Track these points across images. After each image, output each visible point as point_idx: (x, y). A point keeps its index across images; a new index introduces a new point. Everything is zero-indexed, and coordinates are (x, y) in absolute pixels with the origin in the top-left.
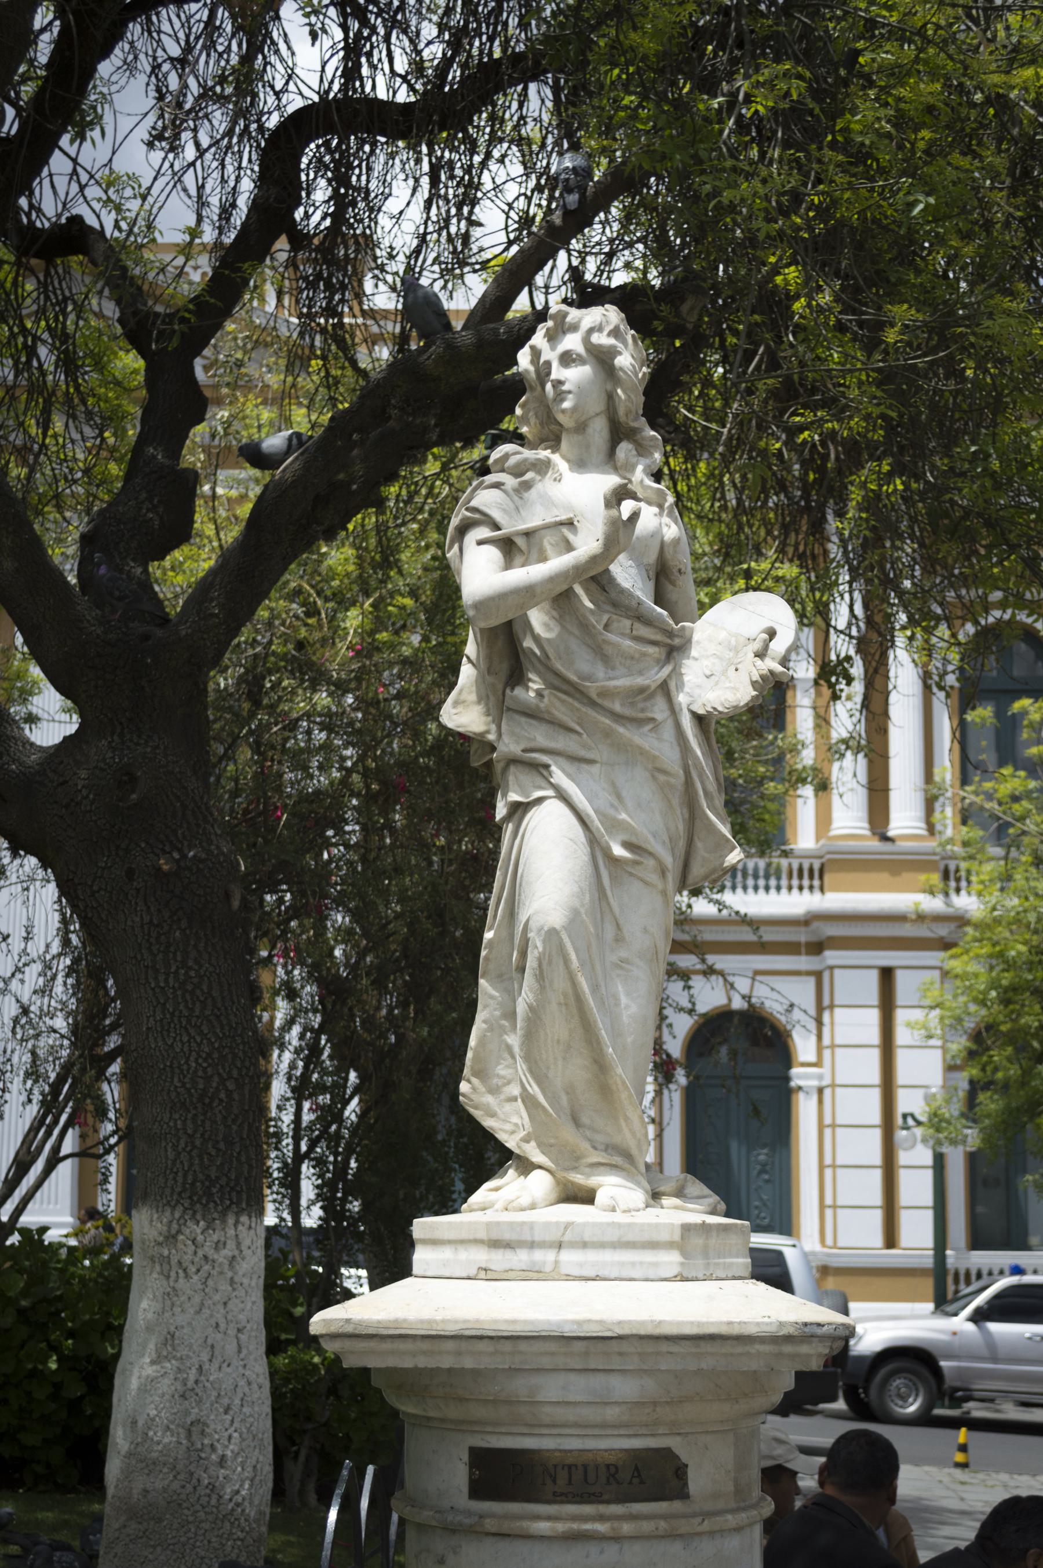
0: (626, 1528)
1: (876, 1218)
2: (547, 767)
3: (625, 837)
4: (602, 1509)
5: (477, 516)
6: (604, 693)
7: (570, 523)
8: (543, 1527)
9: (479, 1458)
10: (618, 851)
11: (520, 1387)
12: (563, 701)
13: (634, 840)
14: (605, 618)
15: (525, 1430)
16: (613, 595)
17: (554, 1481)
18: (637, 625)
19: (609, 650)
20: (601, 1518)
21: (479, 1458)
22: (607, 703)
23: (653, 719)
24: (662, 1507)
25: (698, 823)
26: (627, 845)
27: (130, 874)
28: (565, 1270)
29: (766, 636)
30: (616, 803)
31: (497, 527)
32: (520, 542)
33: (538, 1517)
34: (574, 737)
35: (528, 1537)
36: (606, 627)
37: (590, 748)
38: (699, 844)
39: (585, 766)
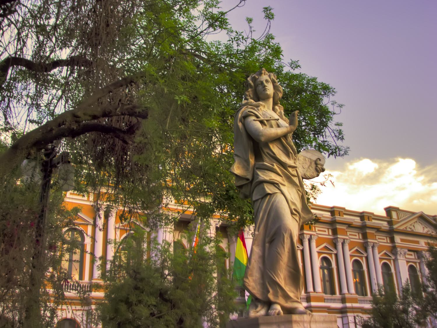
2: (277, 184)
12: (278, 166)
31: (257, 117)
32: (266, 122)
37: (284, 181)
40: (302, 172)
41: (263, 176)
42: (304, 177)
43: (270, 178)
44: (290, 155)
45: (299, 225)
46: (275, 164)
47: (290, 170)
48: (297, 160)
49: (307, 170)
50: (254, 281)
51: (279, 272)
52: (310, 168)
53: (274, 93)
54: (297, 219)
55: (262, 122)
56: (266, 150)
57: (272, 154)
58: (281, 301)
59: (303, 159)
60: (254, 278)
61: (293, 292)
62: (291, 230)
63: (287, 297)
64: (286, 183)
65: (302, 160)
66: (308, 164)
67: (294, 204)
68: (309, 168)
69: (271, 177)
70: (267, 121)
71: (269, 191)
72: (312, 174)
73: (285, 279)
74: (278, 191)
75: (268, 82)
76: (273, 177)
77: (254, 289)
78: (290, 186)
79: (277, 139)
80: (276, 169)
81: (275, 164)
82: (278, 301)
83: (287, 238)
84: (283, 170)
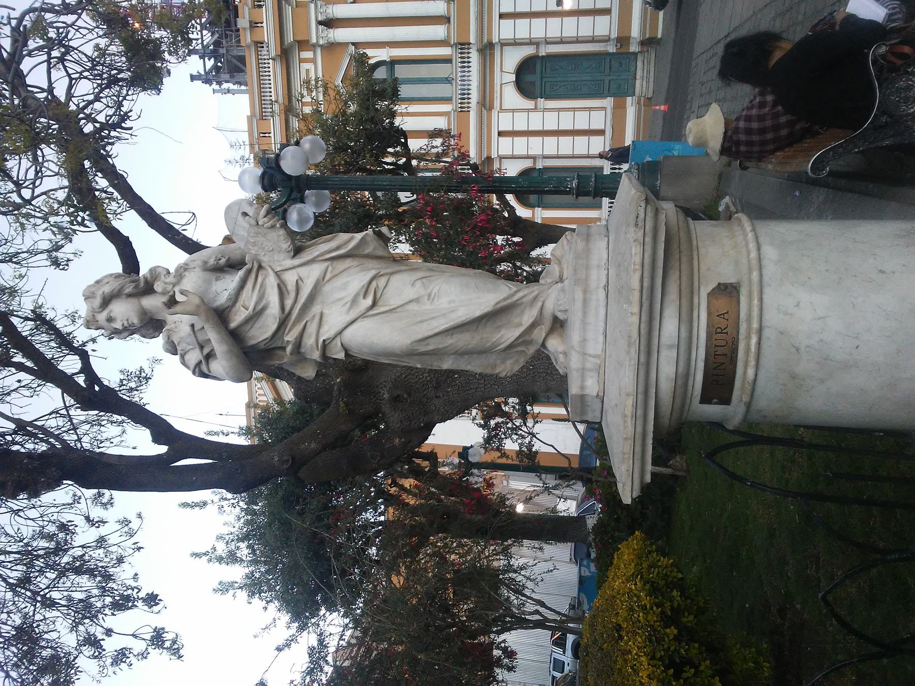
0: (755, 325)
1: (598, 19)
2: (324, 341)
3: (361, 297)
4: (742, 336)
5: (197, 370)
6: (282, 308)
7: (193, 326)
8: (751, 372)
9: (706, 399)
10: (369, 301)
11: (666, 387)
12: (289, 332)
13: (362, 294)
15: (691, 378)
16: (230, 304)
17: (723, 364)
19: (260, 307)
20: (748, 338)
21: (706, 399)
22: (287, 308)
24: (743, 299)
25: (356, 252)
26: (365, 297)
27: (437, 397)
28: (599, 352)
30: (343, 302)
33: (745, 373)
34: (309, 324)
35: (755, 380)
37: (314, 316)
38: (366, 252)
39: (325, 319)
40: (282, 256)
41: (316, 355)
45: (391, 274)
46: (286, 339)
47: (289, 303)
50: (503, 362)
51: (488, 345)
53: (130, 295)
54: (382, 282)
55: (209, 357)
56: (262, 346)
58: (539, 334)
60: (498, 362)
61: (522, 312)
63: (533, 326)
64: (316, 309)
65: (256, 248)
67: (354, 301)
70: (202, 347)
71: (341, 356)
72: (282, 238)
73: (499, 328)
74: (338, 342)
76: (309, 341)
77: (517, 361)
78: (319, 299)
79: (235, 336)
80: (296, 339)
81: (286, 339)
82: (541, 341)
83: (428, 344)
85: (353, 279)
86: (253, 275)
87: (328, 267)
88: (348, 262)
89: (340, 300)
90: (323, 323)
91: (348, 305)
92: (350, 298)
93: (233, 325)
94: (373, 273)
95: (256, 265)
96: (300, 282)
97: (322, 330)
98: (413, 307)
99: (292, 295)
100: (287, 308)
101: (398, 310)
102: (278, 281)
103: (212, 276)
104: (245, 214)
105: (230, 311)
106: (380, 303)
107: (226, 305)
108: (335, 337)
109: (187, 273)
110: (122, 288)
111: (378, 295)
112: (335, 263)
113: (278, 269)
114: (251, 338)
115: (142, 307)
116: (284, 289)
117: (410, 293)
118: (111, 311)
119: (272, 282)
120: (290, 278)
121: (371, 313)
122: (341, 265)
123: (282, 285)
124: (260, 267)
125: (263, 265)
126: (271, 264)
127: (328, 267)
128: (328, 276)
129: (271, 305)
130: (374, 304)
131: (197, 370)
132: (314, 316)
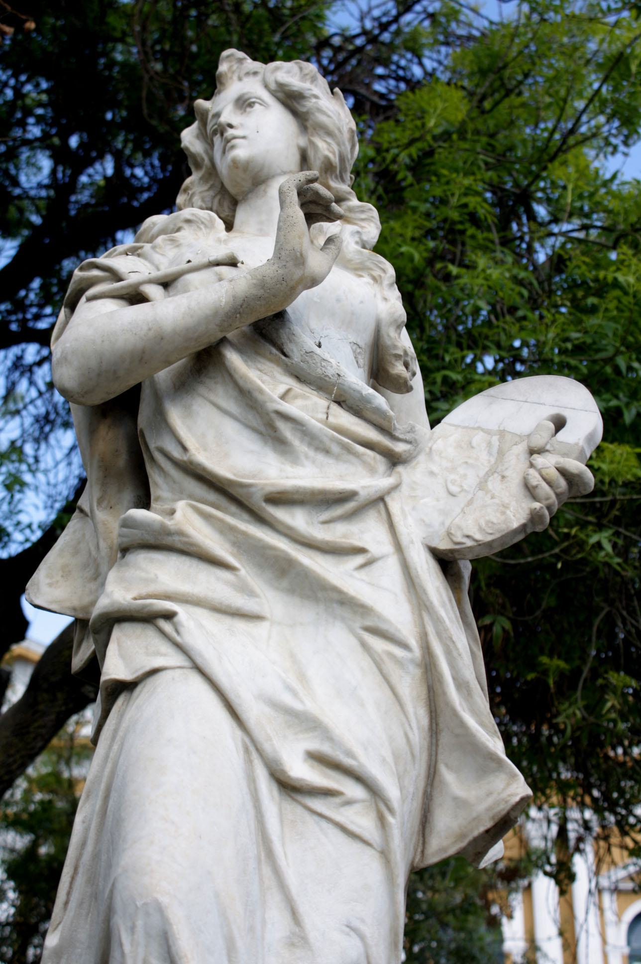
2: (169, 616)
3: (315, 745)
6: (280, 499)
10: (300, 770)
12: (207, 517)
13: (326, 748)
14: (282, 389)
16: (296, 357)
18: (335, 408)
19: (286, 430)
23: (361, 551)
25: (445, 739)
29: (552, 426)
32: (153, 291)
36: (283, 397)
37: (252, 594)
38: (448, 776)
39: (241, 625)
42: (444, 545)
43: (144, 591)
44: (281, 425)
45: (385, 854)
46: (182, 506)
47: (297, 519)
48: (422, 458)
49: (470, 503)
52: (494, 484)
57: (176, 453)
59: (459, 446)
62: (160, 909)
64: (270, 600)
66: (484, 460)
68: (482, 485)
69: (155, 580)
71: (114, 668)
72: (495, 517)
75: (251, 105)
80: (181, 533)
81: (182, 506)
84: (232, 529)
85: (373, 724)
86: (372, 434)
87: (405, 646)
88: (418, 715)
89: (302, 677)
90: (228, 621)
91: (288, 700)
92: (308, 705)
93: (233, 358)
94: (392, 791)
95: (400, 448)
96: (360, 560)
97: (202, 614)
98: (277, 924)
99: (321, 534)
100: (280, 514)
101: (267, 871)
102: (364, 495)
103: (365, 339)
104: (559, 423)
105: (278, 362)
106: (292, 809)
107: (289, 347)
108: (180, 647)
109: (367, 279)
110: (329, 133)
111: (317, 804)
112: (417, 672)
113: (394, 505)
114: (188, 413)
115: (273, 177)
116: (339, 511)
117: (324, 916)
118: (263, 103)
119: (362, 477)
120: (369, 533)
121: (262, 775)
122: (409, 685)
123: (350, 506)
124: (394, 460)
125: (400, 469)
126: (404, 488)
127: (405, 646)
128: (379, 645)
129: (289, 469)
130: (289, 788)
131: (95, 273)
132: (252, 594)
